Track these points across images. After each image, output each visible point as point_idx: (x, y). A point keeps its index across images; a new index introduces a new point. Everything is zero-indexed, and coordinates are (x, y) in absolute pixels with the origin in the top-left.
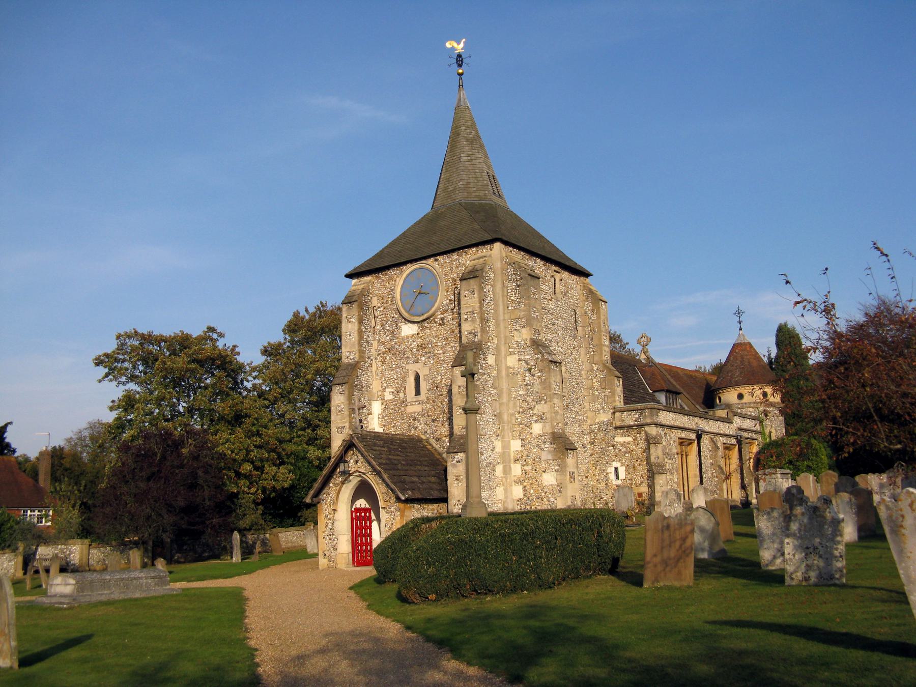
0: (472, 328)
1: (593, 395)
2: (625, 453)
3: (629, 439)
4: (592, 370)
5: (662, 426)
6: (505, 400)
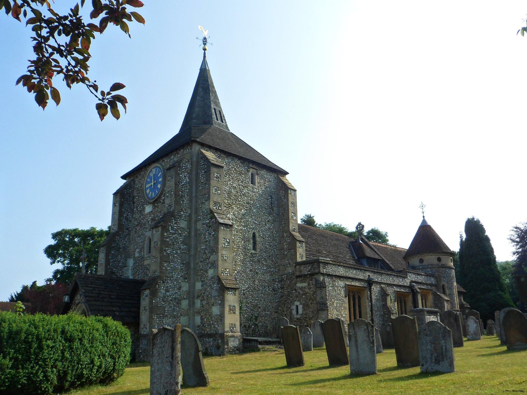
0: (170, 202)
1: (283, 254)
2: (303, 295)
3: (305, 285)
4: (283, 236)
6: (192, 253)
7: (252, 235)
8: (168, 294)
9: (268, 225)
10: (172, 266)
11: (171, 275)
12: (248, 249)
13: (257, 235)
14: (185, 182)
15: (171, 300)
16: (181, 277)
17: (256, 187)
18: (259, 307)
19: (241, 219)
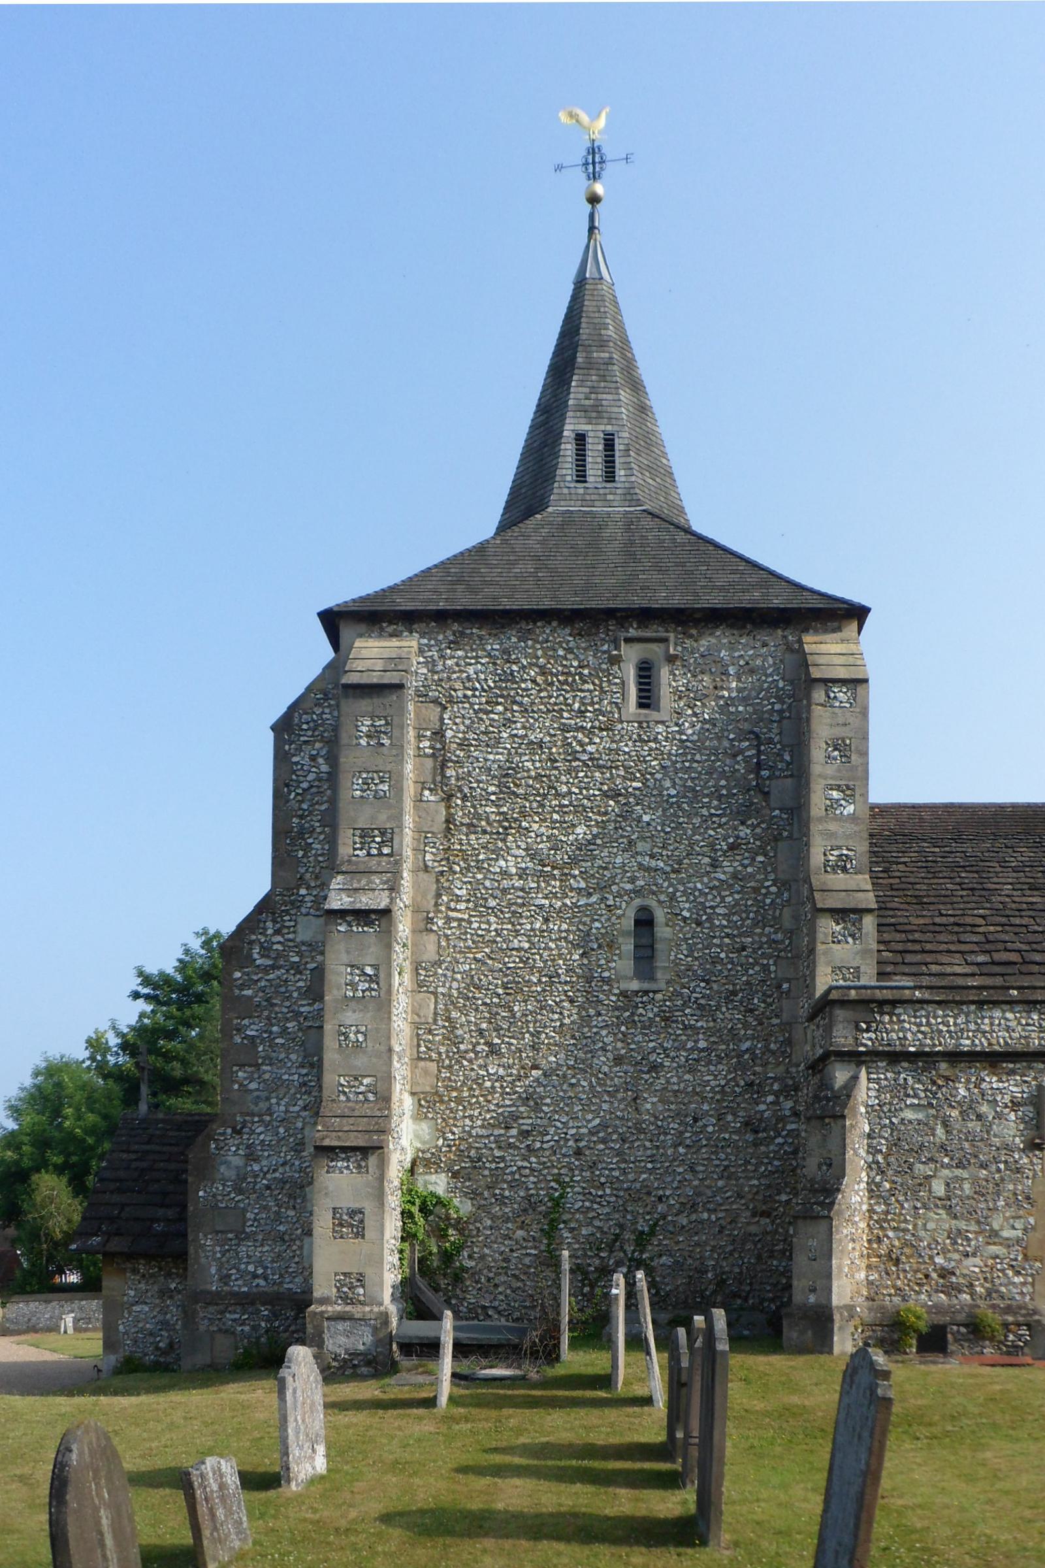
5: (896, 1057)
7: (629, 923)
8: (256, 1167)
9: (728, 867)
10: (267, 1076)
11: (263, 1105)
12: (603, 979)
13: (660, 915)
14: (311, 777)
15: (268, 1187)
16: (305, 1108)
17: (664, 715)
18: (660, 1199)
19: (574, 861)
